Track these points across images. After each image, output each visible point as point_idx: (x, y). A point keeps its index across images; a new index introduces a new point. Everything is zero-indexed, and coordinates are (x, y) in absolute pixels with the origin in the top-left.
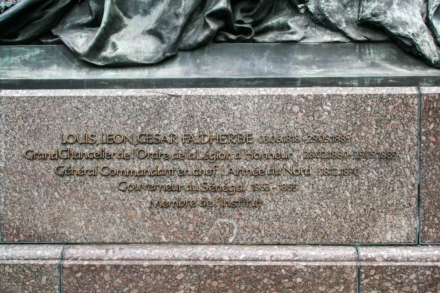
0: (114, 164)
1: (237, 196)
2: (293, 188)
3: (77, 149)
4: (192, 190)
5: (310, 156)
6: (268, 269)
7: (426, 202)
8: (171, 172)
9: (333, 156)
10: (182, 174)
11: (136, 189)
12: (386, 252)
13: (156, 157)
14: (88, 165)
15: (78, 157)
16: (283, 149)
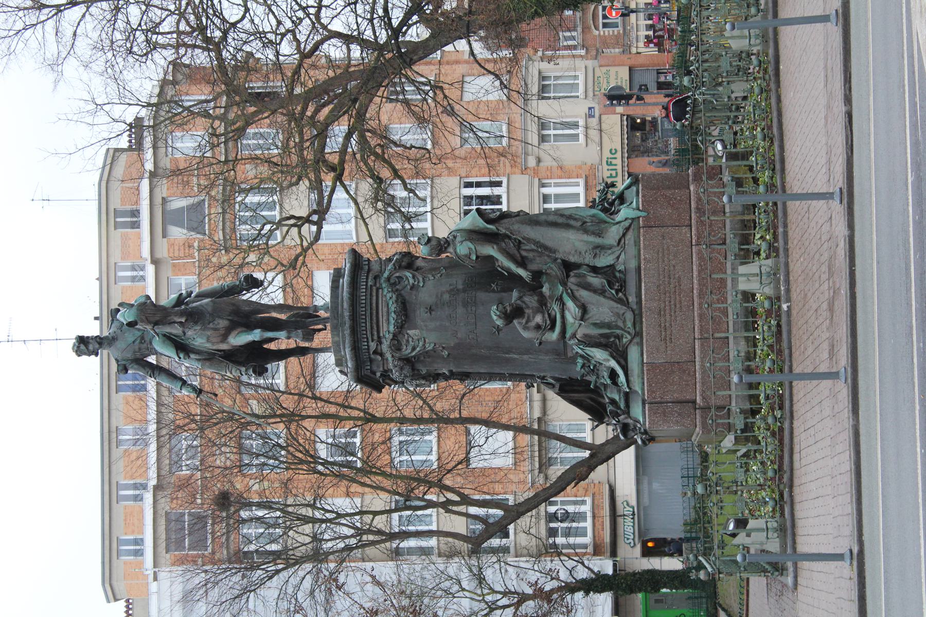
0: (668, 325)
1: (677, 284)
2: (674, 266)
3: (663, 337)
6: (699, 273)
7: (677, 224)
9: (663, 255)
10: (670, 302)
12: (694, 237)
13: (665, 311)
14: (668, 333)
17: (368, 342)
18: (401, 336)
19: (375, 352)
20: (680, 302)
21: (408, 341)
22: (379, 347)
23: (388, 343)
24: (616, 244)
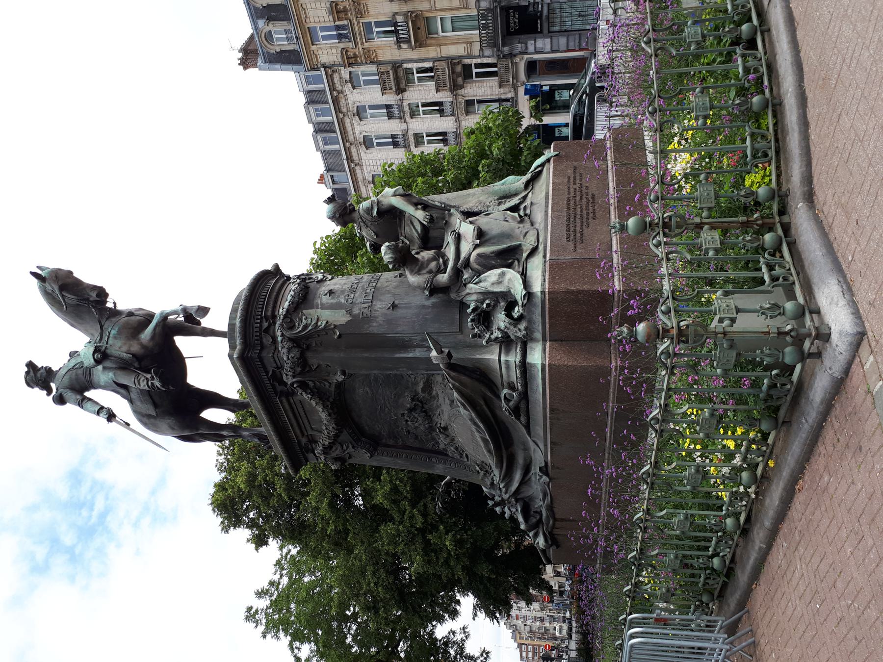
0: (578, 229)
4: (588, 210)
5: (575, 184)
8: (581, 215)
11: (588, 224)
14: (578, 235)
15: (575, 238)
16: (572, 191)
17: (261, 318)
18: (296, 314)
19: (267, 331)
20: (594, 212)
21: (301, 320)
22: (272, 329)
23: (281, 321)
24: (522, 186)
